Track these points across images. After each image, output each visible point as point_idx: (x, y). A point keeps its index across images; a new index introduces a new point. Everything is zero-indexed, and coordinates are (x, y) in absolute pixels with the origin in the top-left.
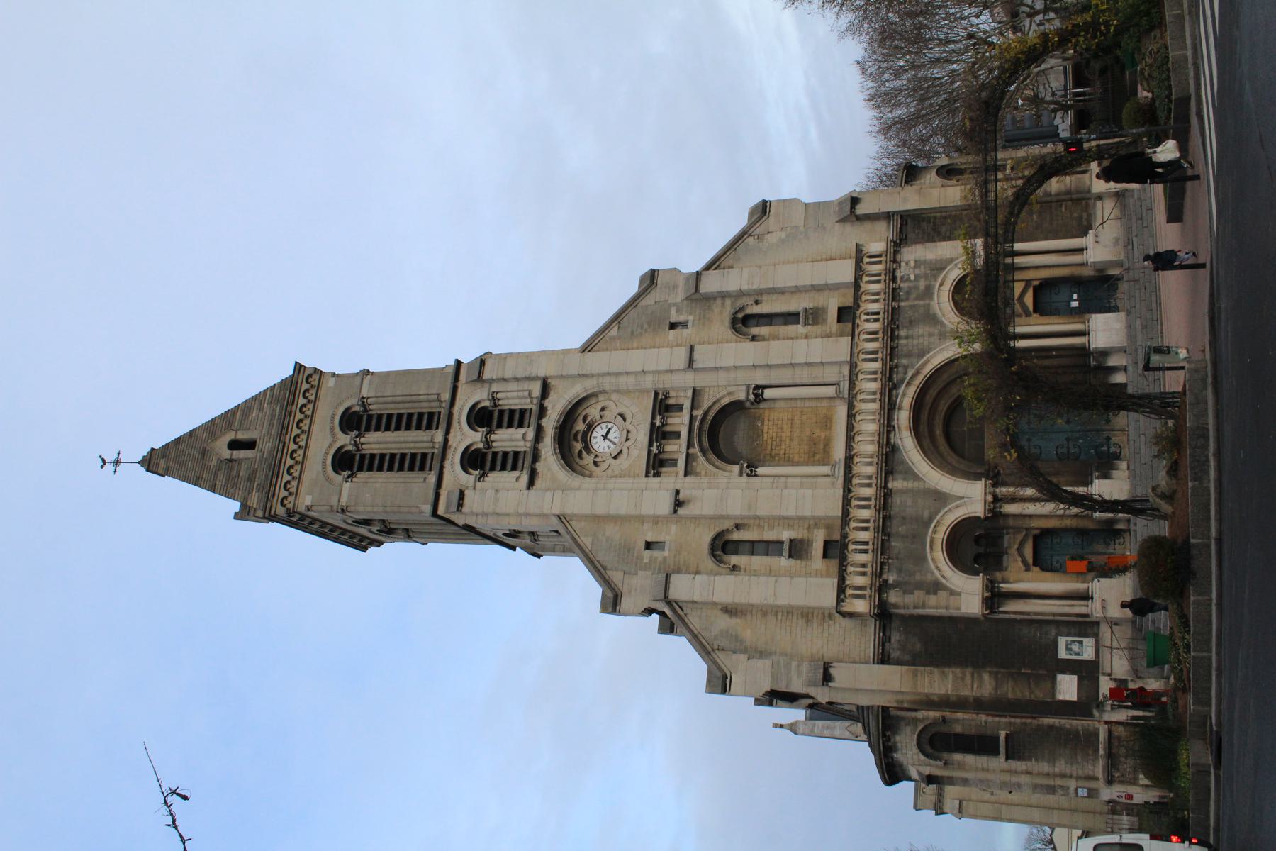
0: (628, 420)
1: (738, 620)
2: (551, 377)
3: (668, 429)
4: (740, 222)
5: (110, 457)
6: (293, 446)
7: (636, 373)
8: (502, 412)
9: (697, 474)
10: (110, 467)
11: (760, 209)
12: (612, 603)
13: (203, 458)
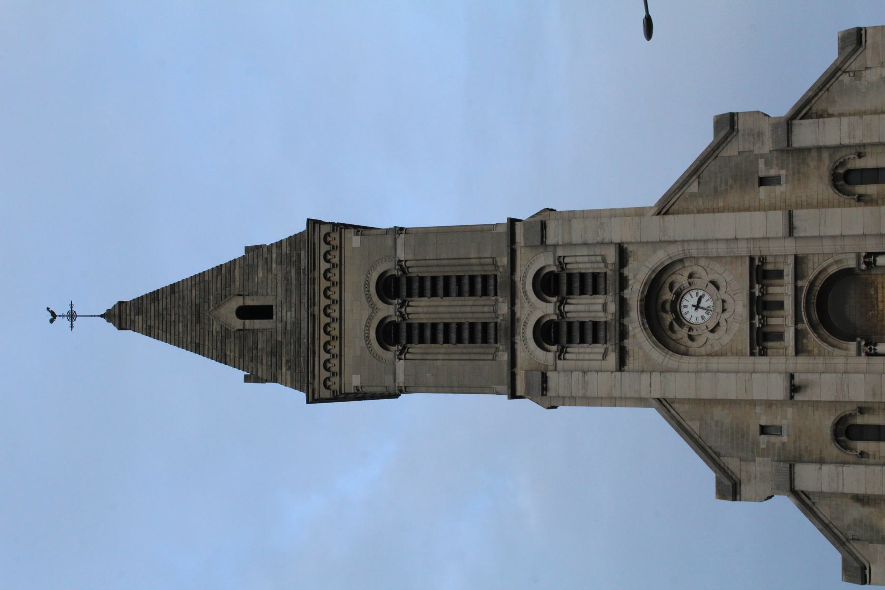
0: (723, 289)
1: (871, 509)
2: (628, 243)
3: (769, 298)
4: (830, 55)
5: (62, 309)
6: (325, 320)
7: (727, 240)
8: (570, 276)
9: (809, 353)
10: (62, 323)
11: (854, 37)
12: (730, 489)
13: (198, 320)
